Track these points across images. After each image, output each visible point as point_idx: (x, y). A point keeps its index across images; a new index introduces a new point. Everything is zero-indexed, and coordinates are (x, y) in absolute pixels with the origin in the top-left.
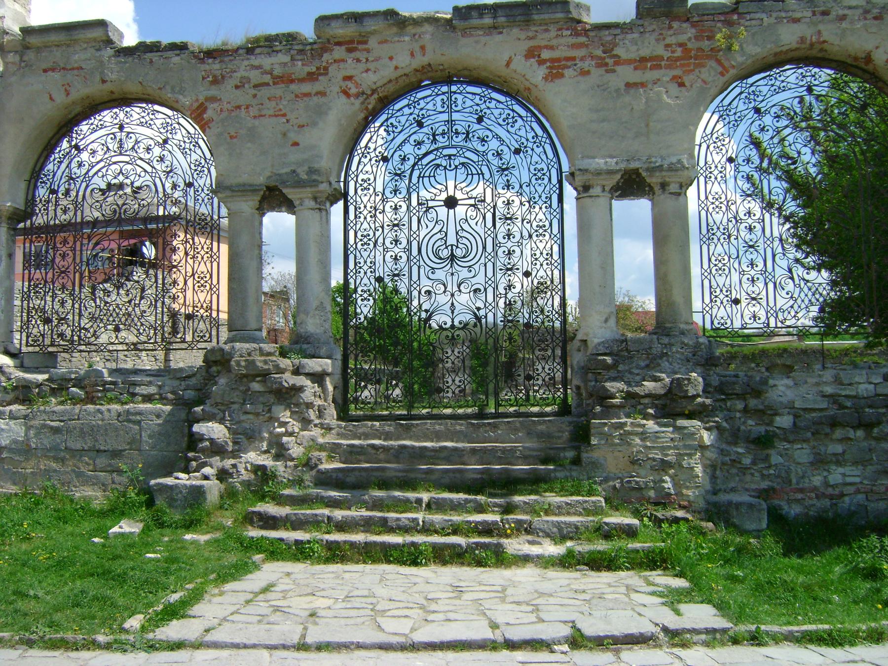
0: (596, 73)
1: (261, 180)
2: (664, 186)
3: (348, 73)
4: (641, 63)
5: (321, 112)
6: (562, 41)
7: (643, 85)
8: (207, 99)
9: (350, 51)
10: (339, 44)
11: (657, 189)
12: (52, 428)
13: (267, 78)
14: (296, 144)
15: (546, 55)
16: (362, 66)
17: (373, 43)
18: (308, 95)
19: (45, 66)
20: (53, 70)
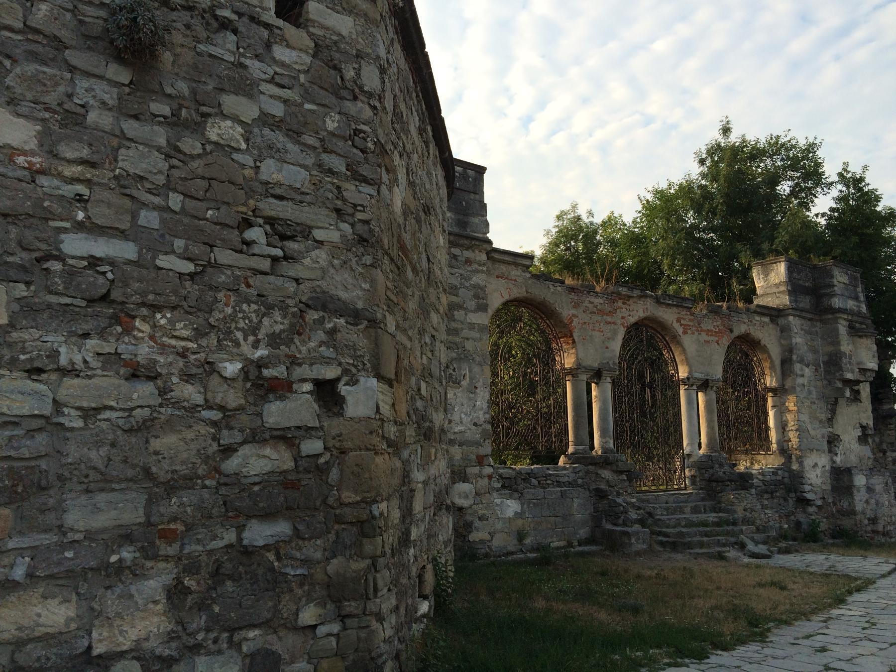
0: (696, 333)
1: (596, 365)
2: (712, 387)
3: (624, 315)
4: (708, 332)
5: (615, 333)
6: (686, 317)
7: (708, 342)
8: (574, 315)
9: (624, 303)
10: (620, 299)
11: (709, 389)
12: (534, 504)
13: (595, 310)
14: (607, 348)
15: (682, 322)
16: (628, 313)
17: (631, 302)
18: (610, 323)
19: (497, 274)
20: (502, 278)
